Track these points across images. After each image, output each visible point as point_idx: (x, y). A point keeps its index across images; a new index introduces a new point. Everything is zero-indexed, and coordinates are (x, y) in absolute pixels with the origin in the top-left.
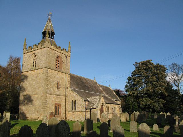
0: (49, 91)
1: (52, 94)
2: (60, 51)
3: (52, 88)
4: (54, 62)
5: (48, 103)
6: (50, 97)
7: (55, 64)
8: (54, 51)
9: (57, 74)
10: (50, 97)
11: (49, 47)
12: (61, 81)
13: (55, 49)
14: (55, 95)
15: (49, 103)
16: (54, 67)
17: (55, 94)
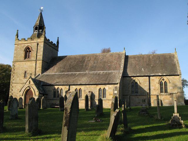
0: (15, 81)
1: (17, 83)
2: (29, 42)
3: (18, 78)
4: (23, 54)
5: (13, 91)
6: (15, 86)
7: (23, 55)
8: (22, 45)
9: (24, 64)
10: (15, 86)
11: (17, 43)
12: (30, 70)
13: (24, 43)
14: (22, 83)
15: (15, 91)
16: (23, 58)
17: (22, 82)
